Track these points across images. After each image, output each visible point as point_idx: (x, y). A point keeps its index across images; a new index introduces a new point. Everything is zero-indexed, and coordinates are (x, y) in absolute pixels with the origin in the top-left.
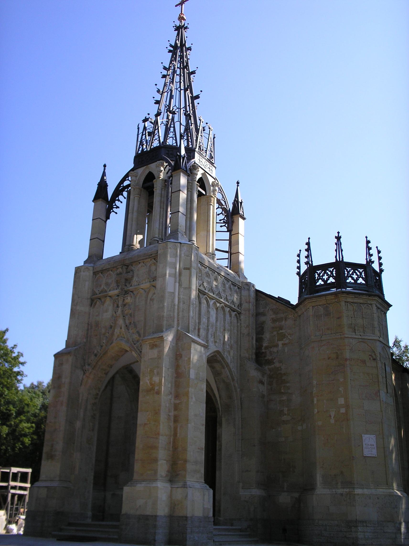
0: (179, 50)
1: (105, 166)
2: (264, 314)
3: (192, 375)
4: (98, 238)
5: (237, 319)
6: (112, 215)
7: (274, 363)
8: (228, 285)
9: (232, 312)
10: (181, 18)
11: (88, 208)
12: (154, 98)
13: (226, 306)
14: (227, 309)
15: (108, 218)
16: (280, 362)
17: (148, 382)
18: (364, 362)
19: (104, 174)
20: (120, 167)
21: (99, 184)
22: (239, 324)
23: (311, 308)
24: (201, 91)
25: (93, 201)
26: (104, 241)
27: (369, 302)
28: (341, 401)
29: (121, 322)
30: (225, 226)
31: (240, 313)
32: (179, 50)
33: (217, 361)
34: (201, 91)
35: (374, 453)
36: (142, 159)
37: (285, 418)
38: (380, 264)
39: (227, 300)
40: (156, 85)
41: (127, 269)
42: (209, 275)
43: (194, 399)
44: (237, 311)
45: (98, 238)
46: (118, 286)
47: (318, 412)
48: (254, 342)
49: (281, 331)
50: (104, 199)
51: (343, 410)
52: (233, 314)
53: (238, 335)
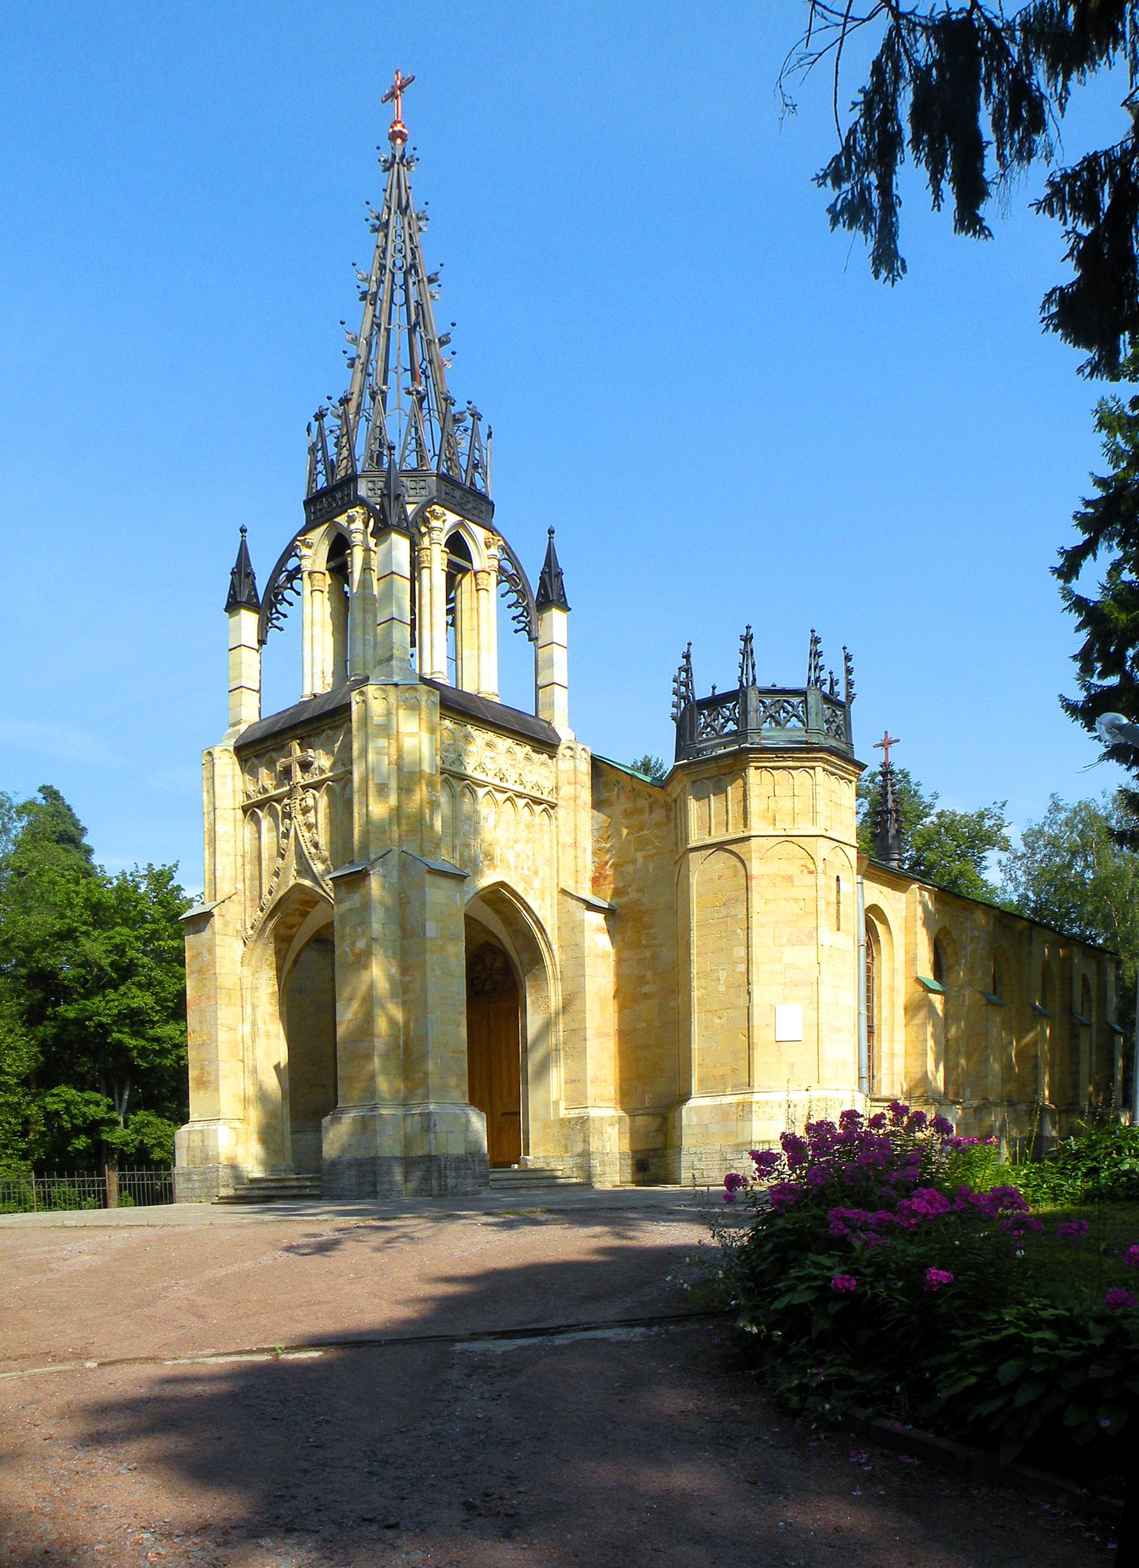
12: (345, 352)
13: (520, 795)
24: (453, 325)
30: (523, 629)
34: (453, 325)
44: (547, 802)
49: (641, 833)
52: (538, 809)
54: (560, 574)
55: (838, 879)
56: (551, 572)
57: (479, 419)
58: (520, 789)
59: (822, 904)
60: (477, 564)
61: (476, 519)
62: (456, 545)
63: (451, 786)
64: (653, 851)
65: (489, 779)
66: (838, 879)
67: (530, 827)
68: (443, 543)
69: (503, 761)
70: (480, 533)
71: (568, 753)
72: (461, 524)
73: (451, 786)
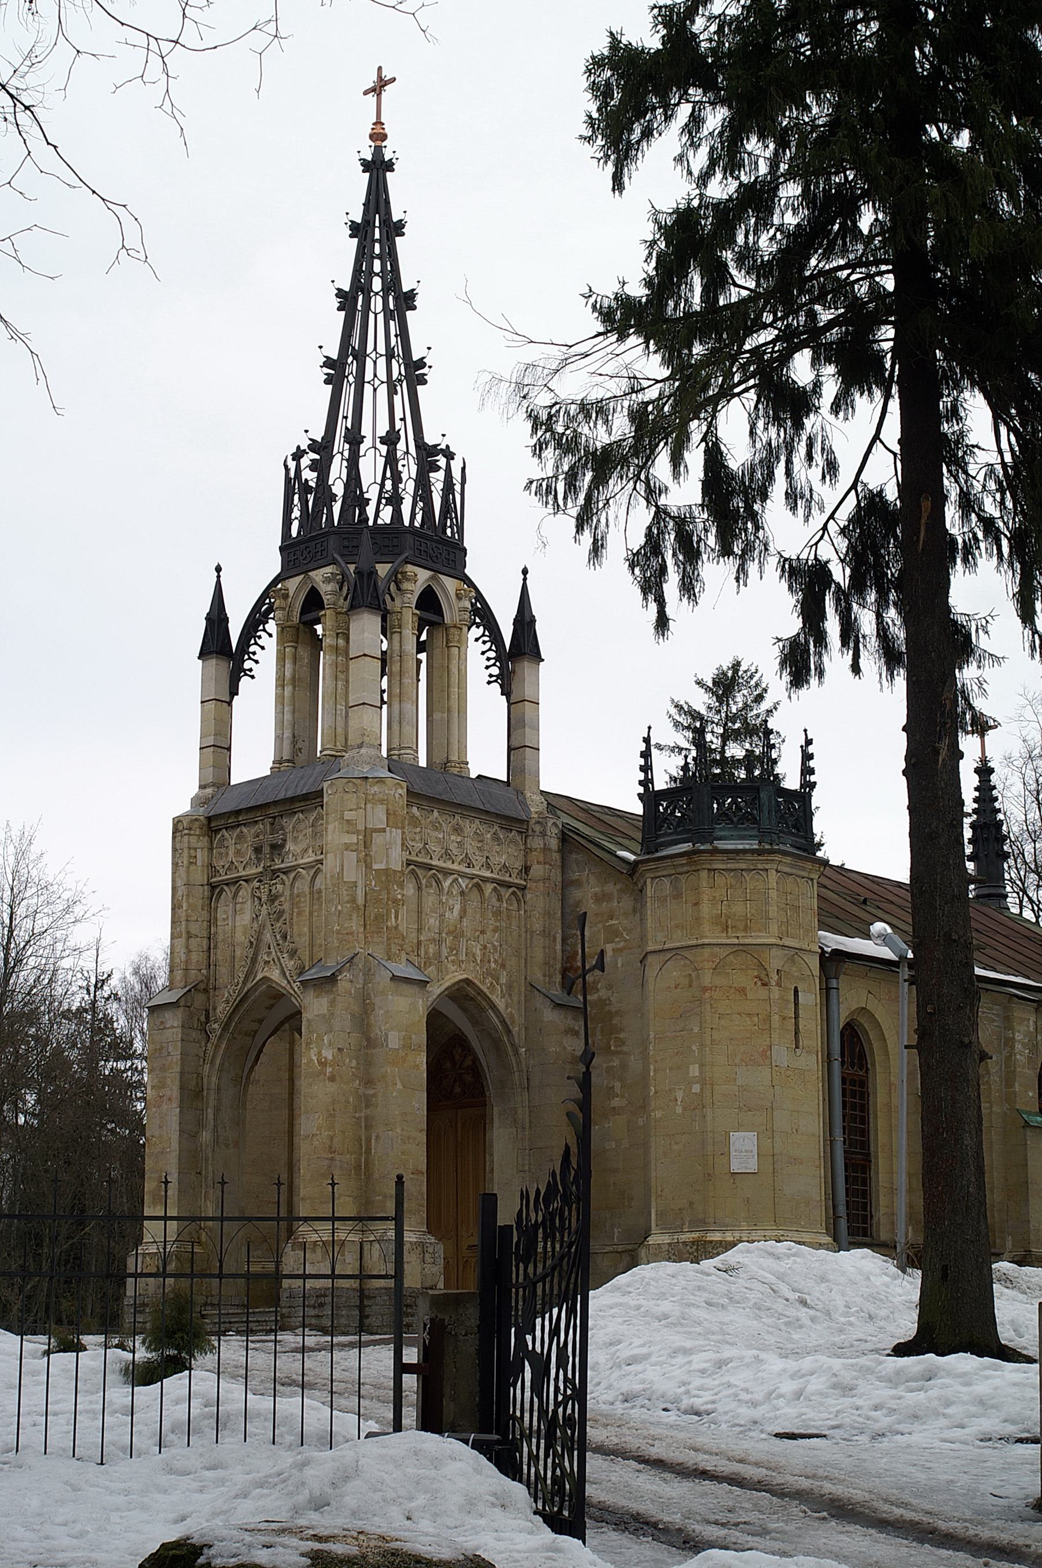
0: (377, 229)
1: (218, 569)
2: (578, 883)
3: (394, 1040)
4: (217, 746)
5: (518, 901)
6: (244, 682)
7: (598, 990)
8: (489, 836)
9: (502, 890)
10: (378, 136)
11: (189, 674)
13: (485, 880)
14: (489, 888)
15: (234, 692)
16: (610, 987)
17: (315, 1058)
18: (742, 991)
19: (218, 585)
20: (253, 566)
21: (209, 618)
22: (522, 912)
23: (649, 880)
25: (201, 656)
26: (229, 749)
27: (760, 866)
28: (694, 1071)
29: (268, 937)
31: (523, 888)
32: (377, 229)
33: (468, 997)
34: (429, 348)
35: (752, 1166)
36: (297, 553)
37: (616, 1102)
38: (807, 771)
39: (488, 867)
40: (321, 347)
41: (272, 824)
42: (441, 825)
43: (399, 1086)
44: (517, 886)
45: (217, 746)
46: (259, 860)
47: (656, 1093)
48: (559, 947)
49: (611, 922)
50: (223, 650)
51: (696, 1088)
52: (506, 893)
53: (520, 936)
54: (533, 620)
55: (796, 991)
56: (525, 621)
57: (453, 459)
58: (488, 874)
59: (776, 1018)
60: (447, 620)
61: (447, 570)
62: (429, 601)
63: (417, 878)
64: (622, 944)
65: (455, 867)
66: (796, 991)
67: (497, 913)
68: (414, 606)
69: (471, 846)
70: (450, 584)
71: (538, 828)
72: (432, 578)
73: (417, 878)
